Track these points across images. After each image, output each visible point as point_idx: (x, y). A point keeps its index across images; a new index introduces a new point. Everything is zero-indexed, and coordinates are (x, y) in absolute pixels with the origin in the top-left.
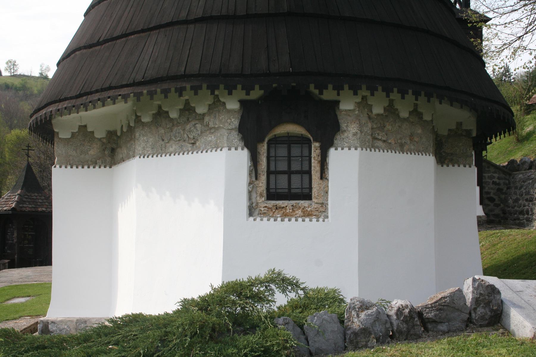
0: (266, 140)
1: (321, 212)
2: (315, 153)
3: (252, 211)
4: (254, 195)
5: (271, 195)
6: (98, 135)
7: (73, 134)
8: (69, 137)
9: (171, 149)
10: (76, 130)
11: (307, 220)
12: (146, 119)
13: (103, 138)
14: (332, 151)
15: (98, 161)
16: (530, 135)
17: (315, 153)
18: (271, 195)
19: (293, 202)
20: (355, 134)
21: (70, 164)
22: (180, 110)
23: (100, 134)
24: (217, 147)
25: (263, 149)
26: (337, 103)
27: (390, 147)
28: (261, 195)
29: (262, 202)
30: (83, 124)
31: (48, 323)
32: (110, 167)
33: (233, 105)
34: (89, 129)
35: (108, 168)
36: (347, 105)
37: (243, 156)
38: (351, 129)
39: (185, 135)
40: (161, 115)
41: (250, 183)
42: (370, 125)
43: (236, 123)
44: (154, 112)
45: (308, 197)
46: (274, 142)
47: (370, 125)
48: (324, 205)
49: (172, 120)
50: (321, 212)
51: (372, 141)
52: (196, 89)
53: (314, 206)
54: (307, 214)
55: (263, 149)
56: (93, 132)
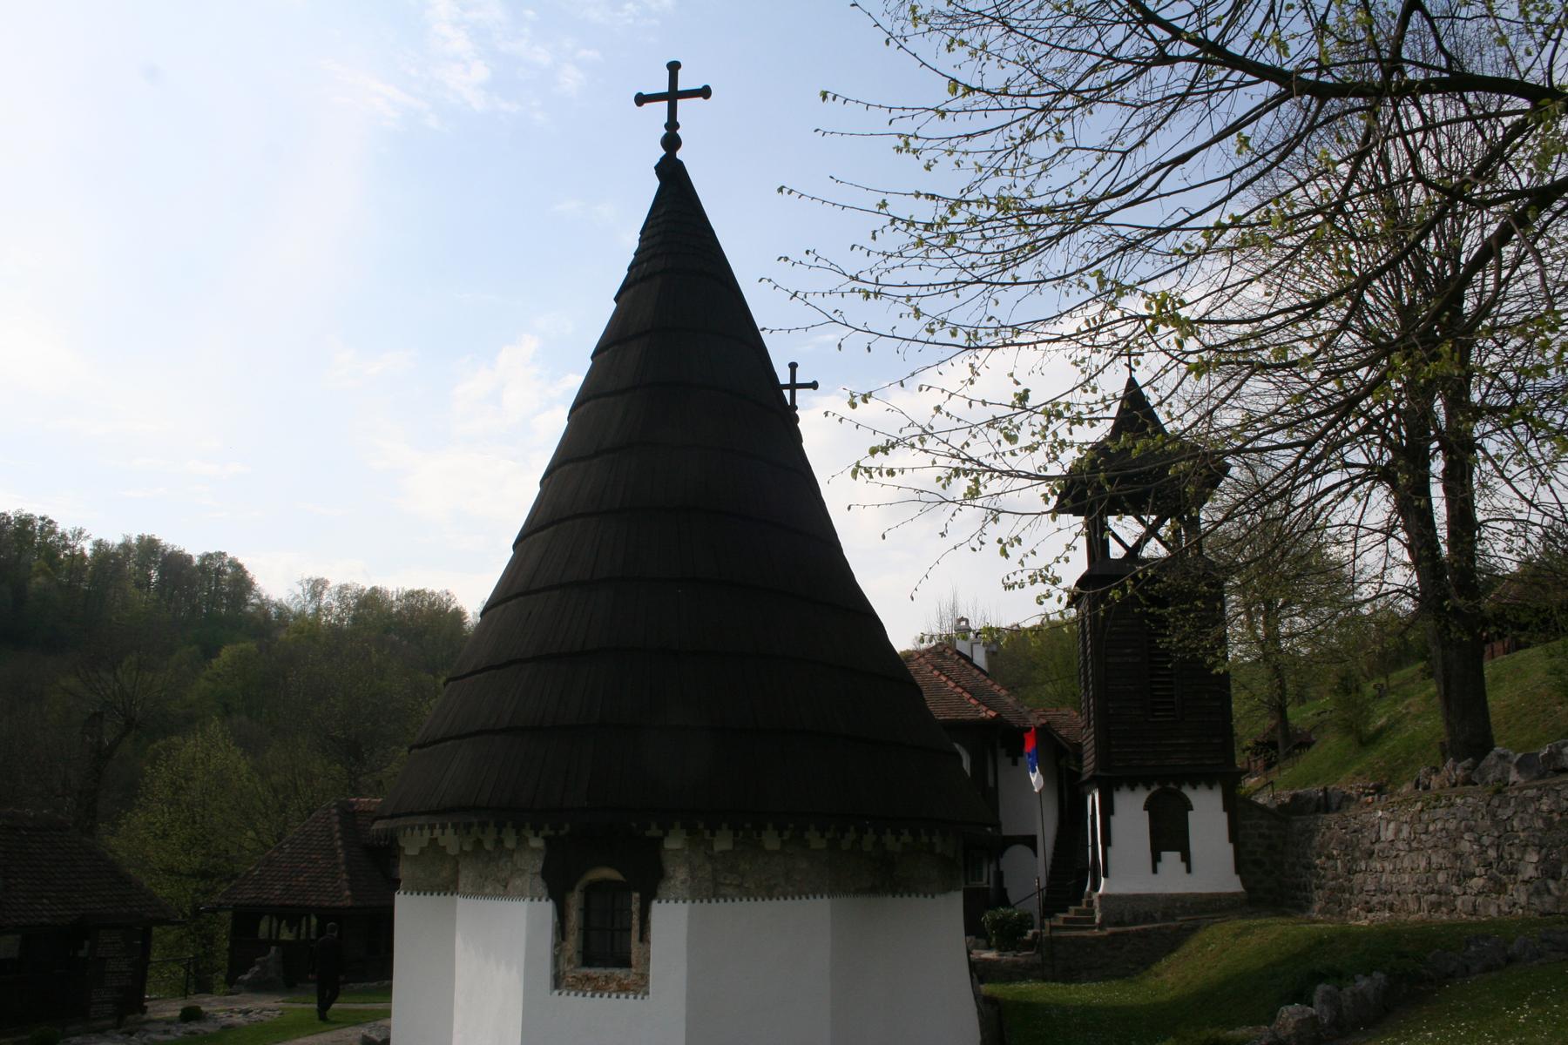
0: (578, 888)
1: (640, 986)
2: (635, 907)
3: (558, 982)
4: (561, 960)
5: (588, 959)
7: (422, 851)
11: (623, 996)
12: (467, 848)
14: (655, 904)
16: (1380, 731)
17: (635, 907)
18: (588, 958)
19: (608, 971)
20: (683, 882)
24: (522, 896)
25: (575, 900)
26: (660, 840)
27: (745, 892)
28: (570, 961)
29: (573, 971)
33: (537, 843)
36: (674, 843)
37: (547, 908)
38: (679, 875)
41: (556, 945)
42: (709, 867)
43: (540, 865)
45: (625, 963)
46: (592, 889)
47: (709, 867)
48: (644, 977)
49: (489, 852)
50: (640, 986)
51: (709, 889)
52: (483, 825)
53: (633, 977)
54: (623, 989)
55: (575, 900)
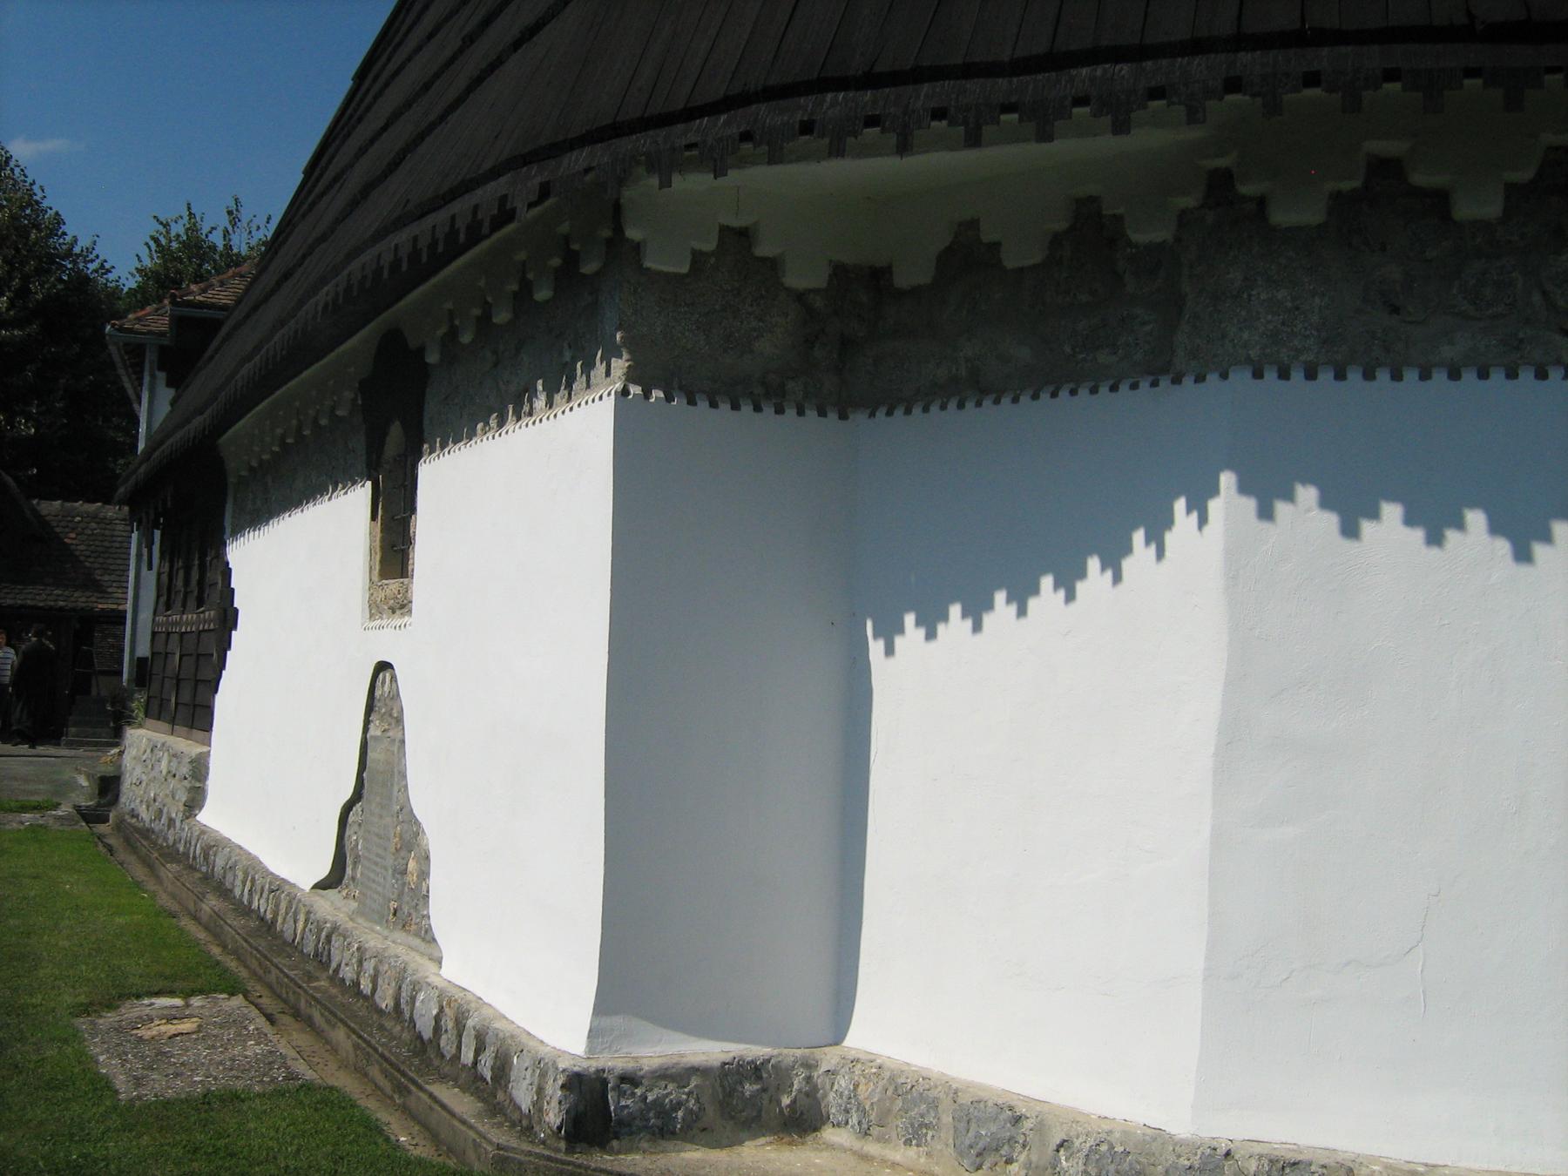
6: (796, 279)
7: (698, 258)
8: (685, 269)
9: (1447, 352)
10: (709, 246)
12: (1298, 211)
13: (816, 291)
15: (790, 385)
21: (681, 388)
22: (1510, 188)
23: (804, 275)
30: (736, 223)
31: (605, 1082)
32: (843, 416)
34: (763, 250)
35: (833, 416)
39: (1536, 298)
40: (1385, 203)
44: (1346, 186)
56: (773, 265)
